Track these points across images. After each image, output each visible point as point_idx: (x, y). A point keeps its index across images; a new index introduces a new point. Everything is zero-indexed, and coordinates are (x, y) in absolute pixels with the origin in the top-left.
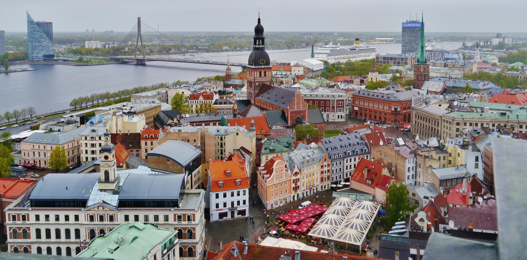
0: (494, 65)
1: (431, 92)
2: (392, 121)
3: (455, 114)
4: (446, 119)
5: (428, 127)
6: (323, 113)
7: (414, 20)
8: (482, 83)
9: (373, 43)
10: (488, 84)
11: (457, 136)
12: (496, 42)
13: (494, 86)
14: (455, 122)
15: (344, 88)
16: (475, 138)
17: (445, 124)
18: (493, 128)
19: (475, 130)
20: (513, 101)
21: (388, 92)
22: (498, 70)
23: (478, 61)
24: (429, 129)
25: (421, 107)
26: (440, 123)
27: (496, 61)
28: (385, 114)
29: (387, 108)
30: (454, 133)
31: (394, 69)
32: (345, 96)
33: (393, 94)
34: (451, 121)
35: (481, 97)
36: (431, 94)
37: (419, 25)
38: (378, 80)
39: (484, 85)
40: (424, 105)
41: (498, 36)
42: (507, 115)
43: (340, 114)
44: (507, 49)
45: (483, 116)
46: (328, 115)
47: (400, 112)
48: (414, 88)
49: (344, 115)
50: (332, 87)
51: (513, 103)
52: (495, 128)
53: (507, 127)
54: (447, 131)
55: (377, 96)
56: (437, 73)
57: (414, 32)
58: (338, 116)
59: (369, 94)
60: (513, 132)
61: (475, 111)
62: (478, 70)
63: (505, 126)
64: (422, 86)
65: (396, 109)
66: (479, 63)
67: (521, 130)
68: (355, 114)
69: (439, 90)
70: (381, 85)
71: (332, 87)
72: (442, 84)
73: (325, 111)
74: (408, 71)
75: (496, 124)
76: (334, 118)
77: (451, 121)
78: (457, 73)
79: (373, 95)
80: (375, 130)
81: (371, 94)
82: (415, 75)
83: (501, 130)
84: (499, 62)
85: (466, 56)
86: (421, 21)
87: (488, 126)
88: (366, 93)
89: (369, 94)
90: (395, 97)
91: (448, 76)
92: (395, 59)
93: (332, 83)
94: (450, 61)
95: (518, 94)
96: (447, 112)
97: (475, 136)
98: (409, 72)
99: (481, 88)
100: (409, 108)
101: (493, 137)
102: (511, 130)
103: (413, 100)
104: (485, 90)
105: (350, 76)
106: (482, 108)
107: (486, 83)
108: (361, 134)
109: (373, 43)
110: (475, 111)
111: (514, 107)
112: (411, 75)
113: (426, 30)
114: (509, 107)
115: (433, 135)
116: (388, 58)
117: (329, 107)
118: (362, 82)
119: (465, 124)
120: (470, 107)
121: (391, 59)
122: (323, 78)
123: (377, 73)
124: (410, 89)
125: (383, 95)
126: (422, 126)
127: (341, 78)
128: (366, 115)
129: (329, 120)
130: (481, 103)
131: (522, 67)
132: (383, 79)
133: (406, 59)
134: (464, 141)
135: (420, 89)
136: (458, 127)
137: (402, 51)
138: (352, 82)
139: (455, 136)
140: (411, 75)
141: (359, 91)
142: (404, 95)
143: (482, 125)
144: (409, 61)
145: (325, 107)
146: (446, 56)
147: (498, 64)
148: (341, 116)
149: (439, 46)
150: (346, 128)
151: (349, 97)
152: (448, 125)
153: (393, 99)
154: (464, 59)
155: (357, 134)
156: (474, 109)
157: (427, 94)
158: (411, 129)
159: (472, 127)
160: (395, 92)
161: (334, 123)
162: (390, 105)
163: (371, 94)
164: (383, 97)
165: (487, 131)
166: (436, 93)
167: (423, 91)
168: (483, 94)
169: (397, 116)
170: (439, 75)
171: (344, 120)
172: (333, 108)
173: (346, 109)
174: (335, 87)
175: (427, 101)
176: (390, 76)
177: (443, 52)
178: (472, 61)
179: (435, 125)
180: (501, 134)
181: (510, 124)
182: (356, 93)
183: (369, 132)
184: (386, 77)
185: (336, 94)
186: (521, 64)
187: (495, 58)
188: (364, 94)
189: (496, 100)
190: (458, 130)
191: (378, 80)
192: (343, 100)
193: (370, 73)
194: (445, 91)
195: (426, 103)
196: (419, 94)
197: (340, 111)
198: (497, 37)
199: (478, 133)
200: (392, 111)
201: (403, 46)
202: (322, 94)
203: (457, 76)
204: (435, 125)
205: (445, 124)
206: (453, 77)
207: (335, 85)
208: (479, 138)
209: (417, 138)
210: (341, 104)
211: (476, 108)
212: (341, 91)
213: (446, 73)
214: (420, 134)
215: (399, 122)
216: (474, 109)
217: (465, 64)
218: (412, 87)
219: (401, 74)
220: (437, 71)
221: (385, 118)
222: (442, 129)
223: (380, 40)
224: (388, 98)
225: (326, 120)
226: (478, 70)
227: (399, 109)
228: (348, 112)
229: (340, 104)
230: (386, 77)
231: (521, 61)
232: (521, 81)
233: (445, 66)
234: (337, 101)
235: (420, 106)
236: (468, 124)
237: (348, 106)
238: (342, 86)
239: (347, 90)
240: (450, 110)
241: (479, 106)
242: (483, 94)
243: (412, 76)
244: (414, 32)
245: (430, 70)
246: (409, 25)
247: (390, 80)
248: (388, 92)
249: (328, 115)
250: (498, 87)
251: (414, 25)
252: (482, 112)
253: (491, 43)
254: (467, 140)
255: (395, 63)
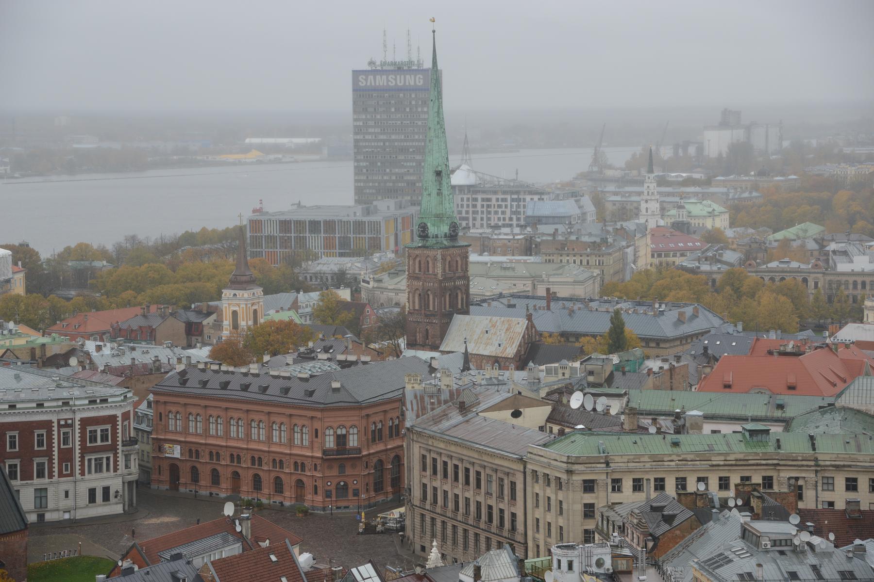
0: (714, 238)
1: (482, 360)
2: (328, 494)
3: (579, 445)
4: (541, 471)
5: (473, 508)
6: (16, 483)
7: (401, 57)
8: (673, 314)
9: (231, 158)
10: (695, 316)
11: (588, 536)
12: (717, 143)
13: (716, 322)
14: (578, 479)
15: (115, 363)
16: (655, 539)
17: (537, 489)
18: (724, 494)
19: (654, 509)
20: (792, 380)
21: (306, 369)
22: (731, 256)
23: (652, 225)
24: (479, 516)
25: (445, 424)
26: (519, 487)
27: (721, 222)
28: (300, 466)
29: (303, 439)
30: (576, 524)
31: (325, 269)
32: (118, 402)
33: (328, 376)
34: (564, 477)
35: (672, 369)
36: (479, 367)
37: (419, 81)
38: (262, 321)
39: (680, 321)
40: (456, 418)
41: (728, 119)
42: (772, 439)
43: (97, 480)
44: (761, 173)
45: (684, 449)
46: (41, 494)
47: (359, 450)
48: (411, 345)
49: (116, 484)
50: (59, 361)
51: (792, 388)
52: (731, 493)
53: (776, 489)
54: (550, 517)
55: (264, 390)
56: (498, 278)
57: (397, 107)
58: (92, 492)
59: (225, 386)
60: (801, 505)
61: (652, 430)
62: (656, 261)
63: (768, 482)
64: (442, 335)
65: (341, 440)
66: (657, 234)
67: (827, 496)
68: (166, 476)
69: (511, 351)
70: (272, 340)
71: (59, 361)
72: (520, 326)
73: (27, 476)
74: (385, 277)
75: (735, 479)
76: (70, 503)
77: (564, 477)
78: (572, 278)
79: (245, 388)
80: (257, 539)
81: (235, 385)
82: (412, 291)
83: (754, 503)
84: (732, 224)
85: (609, 207)
86: (428, 64)
87: (702, 487)
88: (215, 383)
89: (225, 386)
90: (336, 390)
91: (541, 291)
92: (330, 225)
93: (54, 343)
94: (547, 229)
95: (809, 353)
96: (543, 437)
97: (658, 532)
98: (389, 283)
99: (670, 332)
100: (395, 431)
101: (724, 532)
102: (792, 499)
103: (409, 397)
104: (684, 339)
105: (138, 310)
106: (678, 416)
107: (689, 311)
108: (198, 562)
109: (231, 158)
110: (652, 430)
111: (795, 406)
112: (397, 291)
113: (455, 99)
114: (781, 407)
115: (494, 539)
116: (299, 223)
117: (49, 453)
118: (193, 333)
119: (617, 485)
120: (633, 412)
121: (314, 226)
122: (11, 325)
123: (259, 291)
124: (397, 353)
125: (287, 384)
126: (451, 505)
127: (97, 321)
128: (215, 478)
129: (48, 517)
130: (675, 394)
131: (821, 243)
132: (285, 316)
133: (375, 227)
134: (614, 557)
135: (435, 348)
136: (589, 498)
137: (359, 191)
138: (150, 335)
139: (581, 537)
140: (396, 292)
141: (183, 373)
142: (372, 381)
143: (681, 483)
144: (387, 238)
145: (27, 454)
146: (535, 207)
147: (730, 233)
148: (106, 490)
149: (501, 168)
150: (126, 542)
151: (136, 405)
152: (550, 492)
153: (333, 398)
154: (601, 217)
155: (181, 563)
156: (646, 421)
157: (466, 368)
158: (408, 523)
159: (641, 497)
160: (334, 366)
161: (74, 525)
162: (317, 425)
163: (235, 385)
164: (286, 390)
165: (702, 511)
166: (497, 361)
167: (445, 361)
168: (678, 358)
169: (349, 471)
170: (504, 287)
171: (118, 509)
172: (66, 456)
173: (127, 458)
174: (73, 361)
175: (467, 399)
176: (310, 299)
177: (517, 191)
178: (630, 225)
179: (501, 496)
180: (756, 517)
181: (785, 474)
182: (171, 380)
183: (233, 549)
184: (295, 306)
185: (76, 392)
186: (814, 229)
187: (718, 208)
188: (204, 384)
189: (729, 378)
190: (589, 511)
191: (262, 321)
192: (112, 419)
193: (227, 293)
194: (531, 352)
195: (463, 408)
196: (432, 370)
197: (99, 469)
198: (724, 124)
199: (669, 519)
200: (325, 452)
201: (358, 171)
202: (10, 397)
203: (580, 291)
204: (501, 496)
205: (537, 489)
206: (563, 292)
207: (72, 352)
208: (675, 540)
209: (434, 556)
210: (104, 438)
211: (655, 415)
212: (95, 377)
213: (536, 279)
214: (444, 539)
215: (356, 493)
216: (646, 421)
217: (604, 241)
218: (402, 342)
219: (355, 292)
220: (498, 272)
221: (300, 484)
222: (532, 510)
223: (262, 148)
224: (311, 393)
225: (32, 518)
226: (656, 261)
227: (353, 442)
228: (134, 468)
229: (99, 438)
230: (295, 306)
231: (817, 219)
232: (817, 299)
233: (529, 247)
234: (85, 422)
235: (437, 420)
236: (627, 484)
237: (133, 442)
238: (104, 354)
239: (129, 376)
240: (556, 429)
241: (665, 408)
242: (678, 358)
243: (403, 298)
244: (397, 107)
245: (472, 270)
246: (381, 81)
247: (311, 315)
248: (306, 369)
249: (41, 494)
250: (731, 329)
251: (400, 81)
252: (678, 432)
253: (700, 149)
254: (626, 552)
255: (329, 245)
